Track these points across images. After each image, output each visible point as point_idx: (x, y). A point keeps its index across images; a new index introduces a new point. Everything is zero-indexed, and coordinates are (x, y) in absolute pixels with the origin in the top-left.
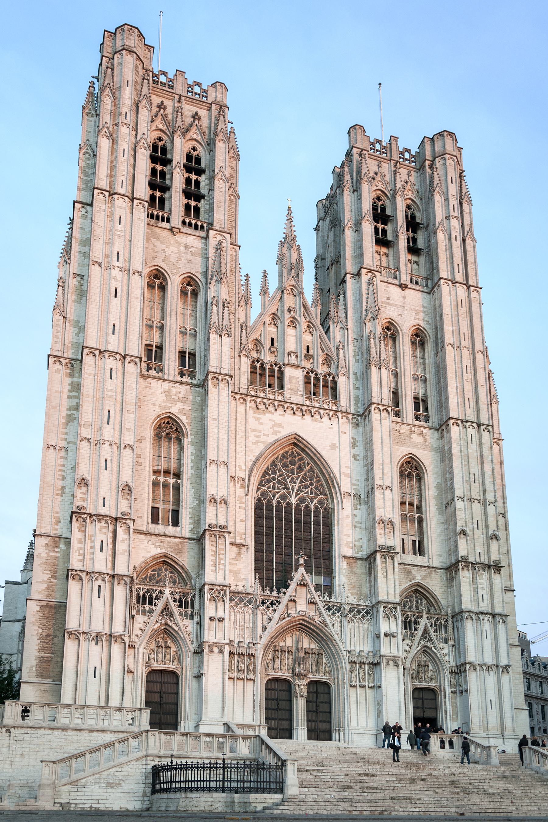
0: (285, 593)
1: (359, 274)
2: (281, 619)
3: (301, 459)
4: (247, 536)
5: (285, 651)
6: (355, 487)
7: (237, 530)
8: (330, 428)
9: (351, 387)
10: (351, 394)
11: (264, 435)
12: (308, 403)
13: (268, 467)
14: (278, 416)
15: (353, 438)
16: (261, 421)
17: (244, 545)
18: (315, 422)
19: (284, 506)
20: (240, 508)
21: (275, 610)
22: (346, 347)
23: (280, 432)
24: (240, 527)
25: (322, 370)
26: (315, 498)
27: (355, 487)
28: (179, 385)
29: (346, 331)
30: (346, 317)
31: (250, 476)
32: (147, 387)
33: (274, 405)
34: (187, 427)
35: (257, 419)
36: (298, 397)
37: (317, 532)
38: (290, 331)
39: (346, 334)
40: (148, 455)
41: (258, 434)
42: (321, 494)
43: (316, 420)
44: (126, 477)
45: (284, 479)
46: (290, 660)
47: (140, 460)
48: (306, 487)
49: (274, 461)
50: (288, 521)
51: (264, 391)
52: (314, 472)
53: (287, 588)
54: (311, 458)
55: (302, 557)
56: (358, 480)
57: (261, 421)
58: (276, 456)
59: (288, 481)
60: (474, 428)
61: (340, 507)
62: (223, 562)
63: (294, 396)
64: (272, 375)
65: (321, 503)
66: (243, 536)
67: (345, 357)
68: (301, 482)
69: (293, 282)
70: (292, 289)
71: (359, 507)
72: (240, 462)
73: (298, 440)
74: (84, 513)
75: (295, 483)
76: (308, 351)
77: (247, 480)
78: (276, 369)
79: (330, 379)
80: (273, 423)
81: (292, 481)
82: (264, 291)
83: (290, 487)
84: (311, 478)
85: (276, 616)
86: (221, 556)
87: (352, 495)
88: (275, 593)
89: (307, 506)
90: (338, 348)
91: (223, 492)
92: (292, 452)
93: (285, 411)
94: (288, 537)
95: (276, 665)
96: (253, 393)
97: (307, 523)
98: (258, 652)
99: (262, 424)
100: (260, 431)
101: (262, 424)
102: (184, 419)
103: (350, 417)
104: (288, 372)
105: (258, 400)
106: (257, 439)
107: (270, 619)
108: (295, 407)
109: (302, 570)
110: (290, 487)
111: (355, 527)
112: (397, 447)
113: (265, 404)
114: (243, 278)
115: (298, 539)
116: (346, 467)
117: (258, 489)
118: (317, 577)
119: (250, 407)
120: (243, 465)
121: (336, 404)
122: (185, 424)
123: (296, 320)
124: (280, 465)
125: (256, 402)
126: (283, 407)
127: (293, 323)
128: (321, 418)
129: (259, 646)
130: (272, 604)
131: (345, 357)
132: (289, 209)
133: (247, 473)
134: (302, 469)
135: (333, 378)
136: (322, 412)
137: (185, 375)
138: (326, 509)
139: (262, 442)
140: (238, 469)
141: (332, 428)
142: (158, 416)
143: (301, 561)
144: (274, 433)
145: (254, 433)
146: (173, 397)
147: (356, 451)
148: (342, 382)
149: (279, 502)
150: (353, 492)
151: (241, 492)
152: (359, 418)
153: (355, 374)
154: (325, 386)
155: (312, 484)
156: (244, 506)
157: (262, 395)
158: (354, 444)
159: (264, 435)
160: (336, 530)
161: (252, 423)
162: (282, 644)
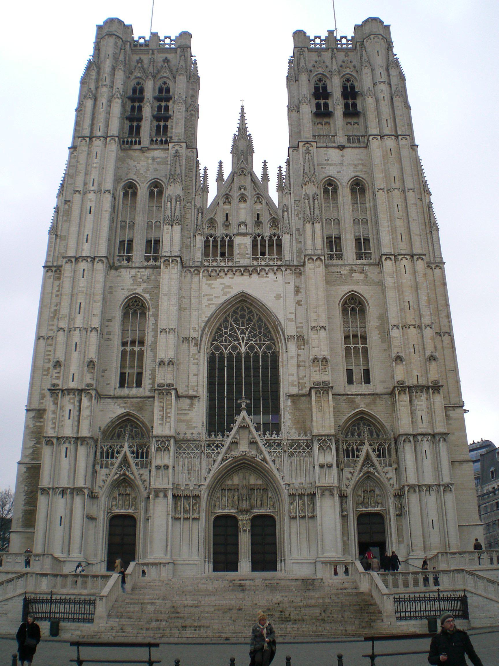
0: (228, 436)
1: (298, 147)
2: (223, 461)
3: (251, 312)
4: (199, 388)
5: (231, 490)
6: (298, 330)
7: (190, 384)
8: (274, 281)
9: (294, 242)
10: (294, 248)
11: (216, 297)
12: (255, 263)
13: (221, 324)
14: (227, 280)
15: (296, 286)
16: (213, 286)
17: (195, 397)
18: (261, 279)
19: (234, 355)
20: (193, 364)
21: (219, 453)
22: (290, 208)
23: (229, 293)
24: (193, 380)
25: (267, 232)
26: (264, 344)
27: (298, 330)
28: (144, 270)
29: (289, 195)
30: (290, 184)
31: (202, 335)
32: (118, 276)
33: (224, 271)
34: (150, 302)
35: (209, 285)
36: (246, 260)
37: (265, 376)
38: (242, 205)
39: (289, 198)
40: (117, 331)
41: (210, 297)
42: (269, 340)
43: (262, 277)
44: (92, 354)
45: (235, 332)
46: (236, 497)
47: (111, 336)
48: (255, 336)
49: (226, 318)
50: (239, 369)
51: (216, 260)
52: (262, 322)
53: (230, 431)
54: (259, 310)
55: (244, 402)
56: (302, 323)
57: (213, 286)
58: (227, 313)
59: (239, 333)
60: (407, 259)
61: (284, 350)
62: (169, 415)
63: (242, 260)
64: (223, 246)
65: (269, 348)
66: (196, 388)
67: (288, 218)
68: (250, 332)
69: (243, 166)
70: (243, 171)
71: (302, 347)
72: (194, 324)
73: (246, 297)
74: (57, 389)
75: (245, 334)
76: (258, 219)
77: (199, 339)
78: (227, 239)
79: (275, 239)
80: (223, 286)
81: (243, 333)
82: (220, 178)
83: (240, 338)
84: (260, 327)
85: (220, 458)
86: (168, 411)
87: (296, 337)
88: (220, 437)
89: (256, 353)
90: (283, 211)
91: (171, 354)
92: (243, 308)
93: (234, 274)
94: (239, 384)
95: (223, 503)
96: (206, 264)
97: (256, 369)
98: (202, 493)
99: (214, 288)
100: (212, 295)
101: (214, 288)
102: (147, 296)
103: (293, 268)
104: (237, 240)
105: (210, 269)
106: (209, 302)
107: (214, 461)
108: (242, 269)
109: (244, 413)
110: (240, 338)
111: (299, 366)
112: (338, 287)
113: (216, 271)
114: (202, 172)
115: (247, 384)
116: (290, 313)
117: (212, 344)
118: (266, 417)
119: (203, 276)
120: (196, 326)
121: (280, 259)
122: (148, 300)
123: (246, 195)
124: (231, 320)
125: (208, 272)
126: (232, 271)
127: (243, 198)
128: (267, 274)
129: (203, 487)
130: (217, 447)
131: (288, 218)
132: (242, 108)
133: (200, 332)
134: (252, 321)
135: (278, 237)
136: (267, 269)
137: (150, 260)
138: (273, 353)
139: (213, 304)
140: (192, 331)
141: (277, 281)
142: (126, 298)
143: (244, 405)
144: (224, 294)
145: (206, 297)
146: (139, 280)
147: (298, 298)
148: (286, 239)
149: (230, 353)
150: (298, 334)
151: (193, 350)
152: (302, 268)
153: (298, 230)
154: (271, 245)
155: (260, 333)
156: (196, 361)
157: (214, 264)
158: (297, 291)
159: (216, 297)
160: (282, 371)
161: (205, 289)
162: (229, 482)
